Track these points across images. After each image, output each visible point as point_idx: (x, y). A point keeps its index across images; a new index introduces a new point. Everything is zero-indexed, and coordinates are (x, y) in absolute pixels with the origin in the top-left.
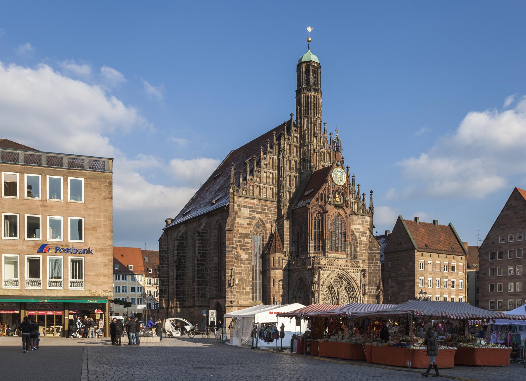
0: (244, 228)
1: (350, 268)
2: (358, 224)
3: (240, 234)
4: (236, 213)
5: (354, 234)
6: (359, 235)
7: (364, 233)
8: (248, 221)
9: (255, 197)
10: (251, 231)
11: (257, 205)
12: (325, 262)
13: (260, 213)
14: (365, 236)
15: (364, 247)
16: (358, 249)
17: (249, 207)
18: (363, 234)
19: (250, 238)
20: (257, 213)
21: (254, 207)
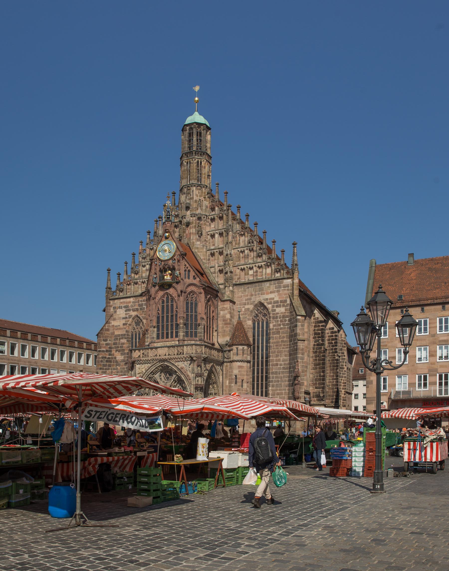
0: (120, 329)
1: (172, 357)
2: (271, 293)
3: (116, 336)
4: (112, 316)
5: (265, 307)
6: (273, 307)
7: (281, 302)
8: (124, 321)
9: (132, 295)
10: (127, 331)
11: (133, 302)
12: (139, 354)
13: (137, 310)
14: (284, 306)
15: (281, 321)
16: (271, 326)
17: (125, 307)
18: (277, 304)
19: (125, 338)
20: (134, 310)
21: (130, 305)
